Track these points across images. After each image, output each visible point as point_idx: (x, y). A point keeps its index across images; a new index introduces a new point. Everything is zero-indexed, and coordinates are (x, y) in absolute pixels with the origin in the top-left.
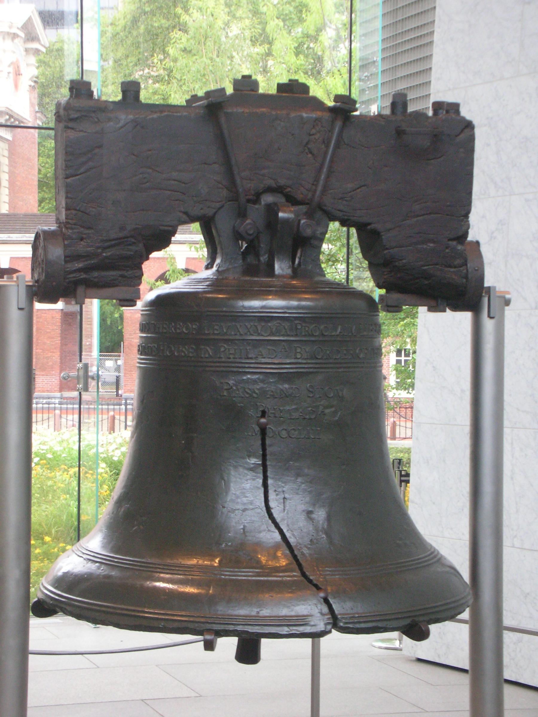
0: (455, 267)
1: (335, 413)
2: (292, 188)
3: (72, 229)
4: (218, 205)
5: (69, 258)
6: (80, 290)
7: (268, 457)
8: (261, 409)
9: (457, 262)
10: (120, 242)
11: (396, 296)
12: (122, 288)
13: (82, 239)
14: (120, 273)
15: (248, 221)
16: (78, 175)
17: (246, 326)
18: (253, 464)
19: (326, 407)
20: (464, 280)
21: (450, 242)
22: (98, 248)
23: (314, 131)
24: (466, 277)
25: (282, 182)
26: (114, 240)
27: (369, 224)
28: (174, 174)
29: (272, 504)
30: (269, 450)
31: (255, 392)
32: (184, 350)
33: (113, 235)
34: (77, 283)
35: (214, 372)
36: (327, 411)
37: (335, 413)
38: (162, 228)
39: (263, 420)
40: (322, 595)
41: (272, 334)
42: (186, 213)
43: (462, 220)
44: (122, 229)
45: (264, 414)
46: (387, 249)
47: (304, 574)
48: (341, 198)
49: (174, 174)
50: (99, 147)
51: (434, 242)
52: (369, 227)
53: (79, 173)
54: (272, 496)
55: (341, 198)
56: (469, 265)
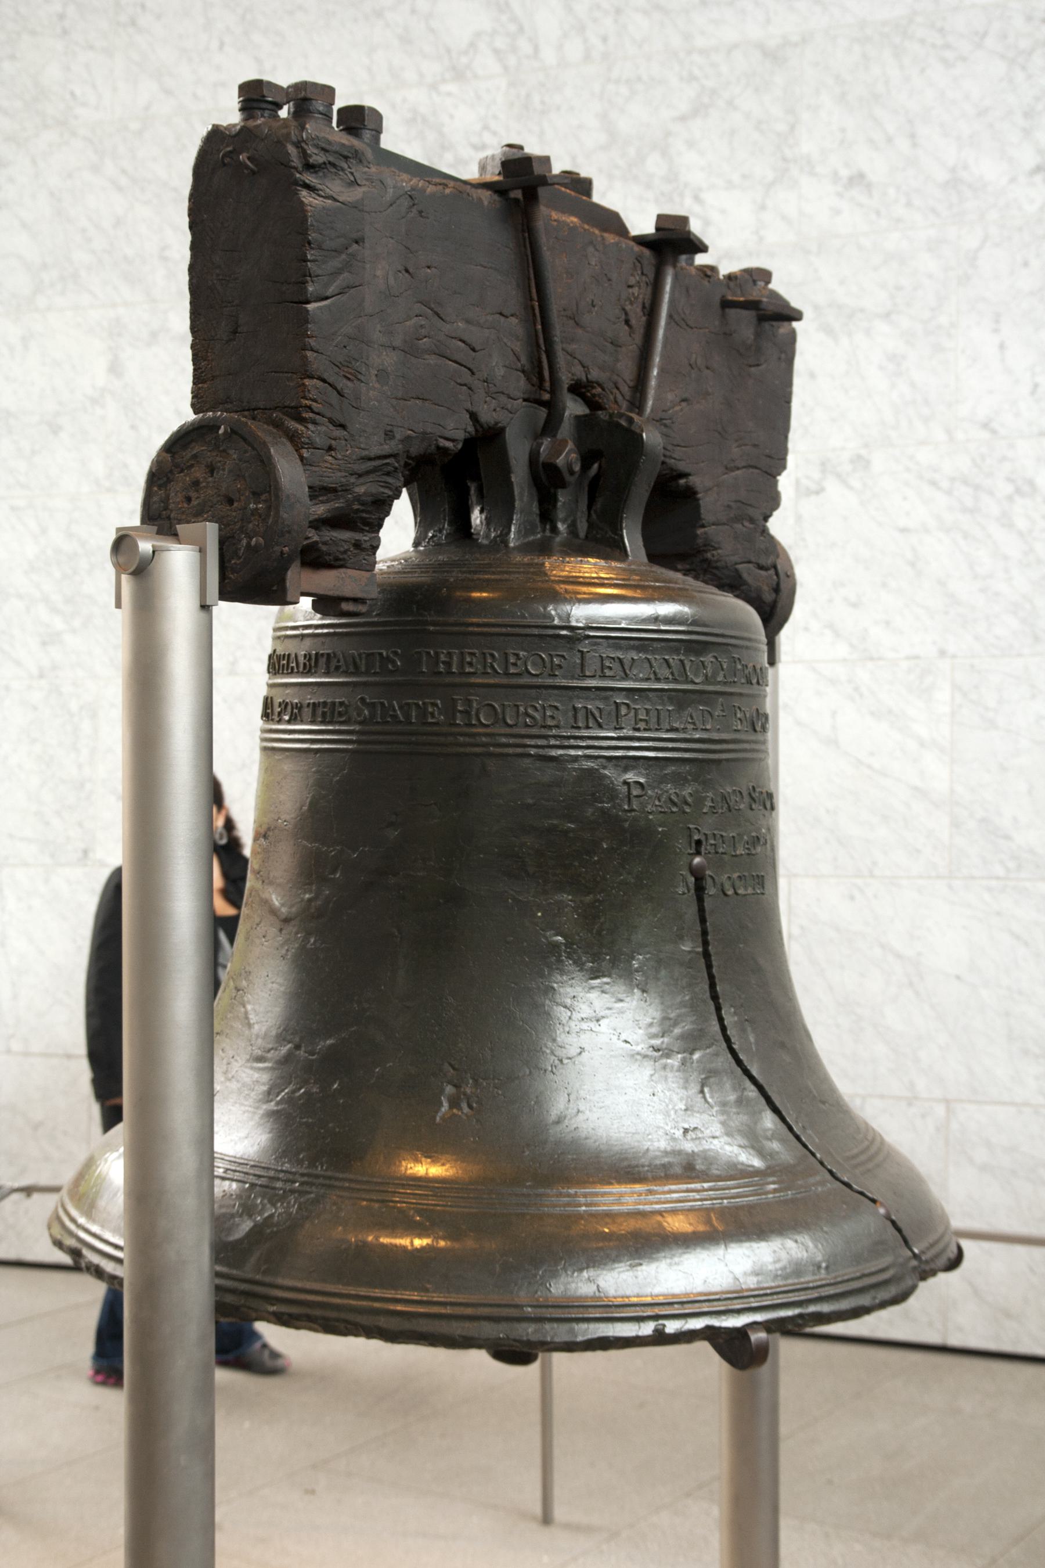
2: (603, 389)
3: (314, 423)
5: (317, 492)
8: (696, 837)
12: (350, 572)
14: (357, 536)
16: (327, 298)
17: (666, 661)
18: (689, 952)
23: (632, 281)
24: (777, 590)
26: (379, 458)
27: (685, 475)
31: (686, 803)
32: (530, 711)
35: (610, 759)
38: (443, 443)
40: (882, 1211)
41: (707, 680)
46: (703, 526)
52: (682, 481)
53: (330, 291)
56: (779, 567)
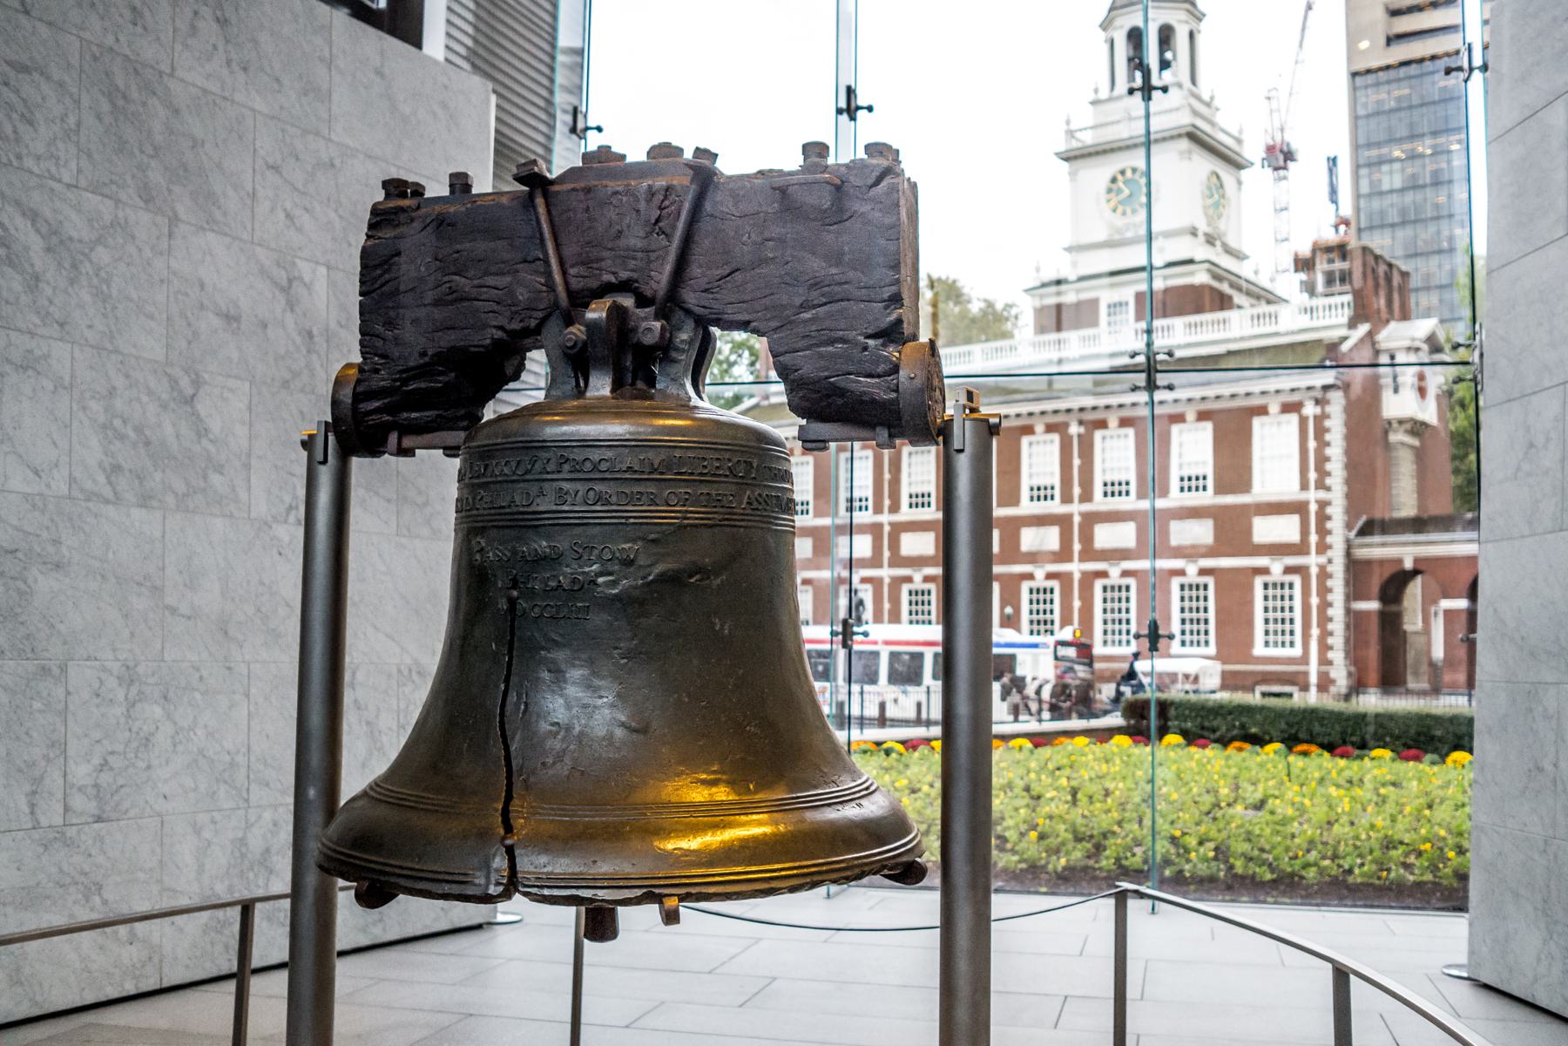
0: (879, 376)
1: (614, 583)
4: (541, 315)
5: (358, 397)
6: (393, 438)
7: (516, 644)
9: (881, 369)
10: (423, 371)
11: (821, 429)
13: (377, 371)
15: (572, 329)
19: (601, 574)
20: (894, 395)
21: (871, 342)
22: (395, 380)
24: (897, 391)
25: (624, 275)
28: (490, 281)
29: (509, 708)
30: (518, 633)
33: (412, 364)
34: (386, 428)
36: (601, 580)
37: (614, 583)
39: (515, 593)
42: (501, 328)
43: (886, 308)
44: (423, 354)
45: (514, 587)
47: (505, 813)
48: (706, 291)
49: (490, 281)
50: (398, 254)
51: (843, 340)
54: (513, 697)
55: (706, 291)
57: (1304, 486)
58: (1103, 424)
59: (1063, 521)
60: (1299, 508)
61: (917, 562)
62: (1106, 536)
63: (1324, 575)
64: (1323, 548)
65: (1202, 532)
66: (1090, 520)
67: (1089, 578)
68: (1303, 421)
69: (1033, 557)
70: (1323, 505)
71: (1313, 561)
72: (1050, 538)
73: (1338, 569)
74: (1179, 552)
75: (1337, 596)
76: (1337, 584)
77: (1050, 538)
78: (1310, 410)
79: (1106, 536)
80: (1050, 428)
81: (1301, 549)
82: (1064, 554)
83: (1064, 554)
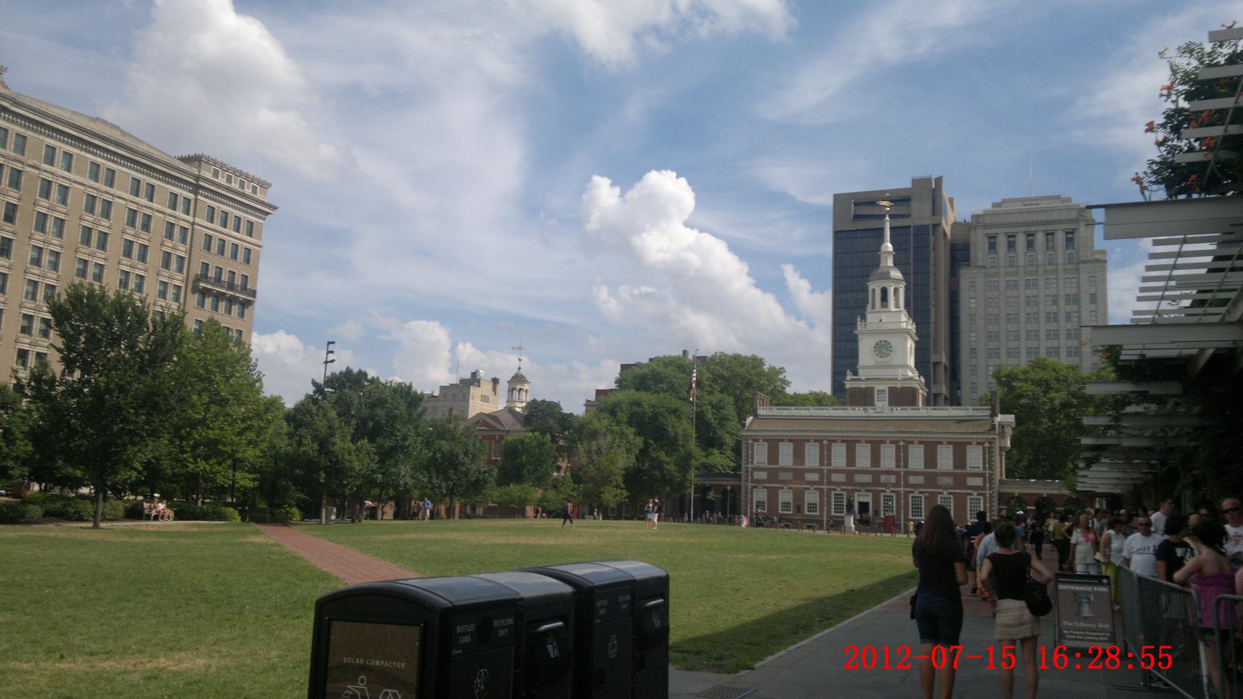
57: (984, 468)
58: (912, 442)
59: (897, 474)
60: (983, 475)
61: (839, 484)
62: (912, 480)
63: (991, 496)
64: (991, 488)
65: (949, 481)
66: (908, 474)
67: (906, 493)
68: (984, 449)
69: (885, 485)
70: (991, 475)
71: (988, 492)
72: (893, 479)
73: (996, 495)
74: (940, 487)
75: (996, 504)
76: (996, 500)
77: (893, 479)
78: (987, 445)
79: (912, 480)
80: (892, 442)
81: (983, 488)
82: (897, 484)
83: (897, 484)
